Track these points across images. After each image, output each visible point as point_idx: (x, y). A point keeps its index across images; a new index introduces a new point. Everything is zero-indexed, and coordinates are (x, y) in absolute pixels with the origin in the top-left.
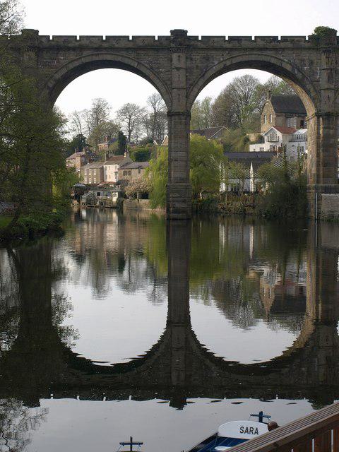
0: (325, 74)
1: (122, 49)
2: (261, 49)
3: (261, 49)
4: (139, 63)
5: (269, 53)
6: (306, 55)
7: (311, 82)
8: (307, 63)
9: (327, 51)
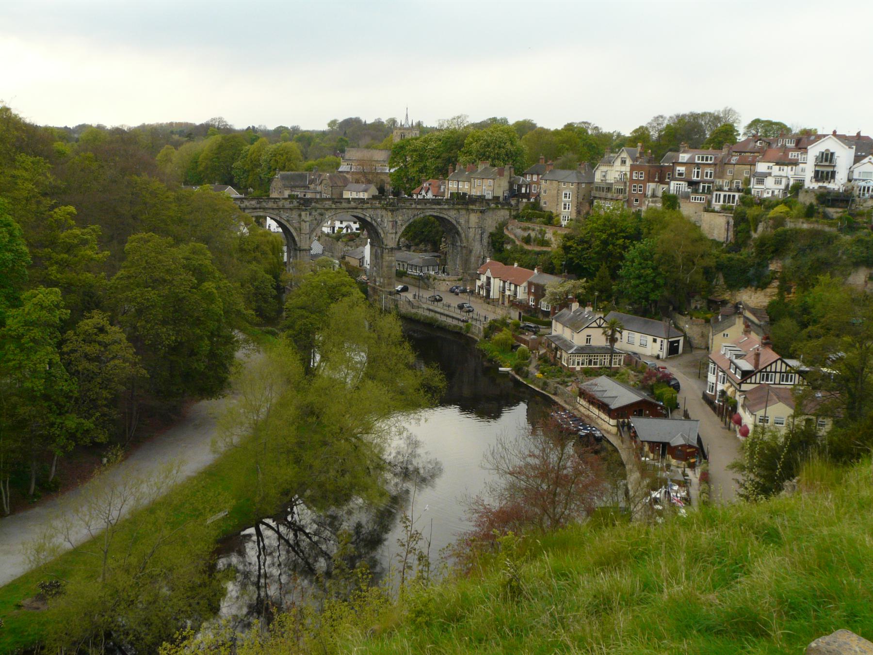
0: (390, 224)
1: (269, 209)
2: (353, 208)
3: (353, 208)
4: (281, 217)
5: (358, 210)
6: (379, 212)
7: (382, 228)
8: (380, 216)
9: (392, 211)
